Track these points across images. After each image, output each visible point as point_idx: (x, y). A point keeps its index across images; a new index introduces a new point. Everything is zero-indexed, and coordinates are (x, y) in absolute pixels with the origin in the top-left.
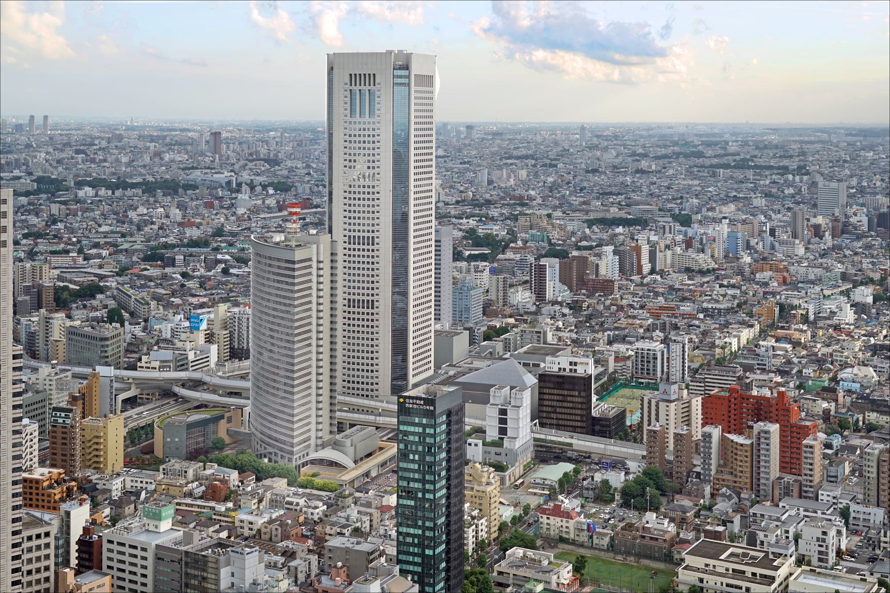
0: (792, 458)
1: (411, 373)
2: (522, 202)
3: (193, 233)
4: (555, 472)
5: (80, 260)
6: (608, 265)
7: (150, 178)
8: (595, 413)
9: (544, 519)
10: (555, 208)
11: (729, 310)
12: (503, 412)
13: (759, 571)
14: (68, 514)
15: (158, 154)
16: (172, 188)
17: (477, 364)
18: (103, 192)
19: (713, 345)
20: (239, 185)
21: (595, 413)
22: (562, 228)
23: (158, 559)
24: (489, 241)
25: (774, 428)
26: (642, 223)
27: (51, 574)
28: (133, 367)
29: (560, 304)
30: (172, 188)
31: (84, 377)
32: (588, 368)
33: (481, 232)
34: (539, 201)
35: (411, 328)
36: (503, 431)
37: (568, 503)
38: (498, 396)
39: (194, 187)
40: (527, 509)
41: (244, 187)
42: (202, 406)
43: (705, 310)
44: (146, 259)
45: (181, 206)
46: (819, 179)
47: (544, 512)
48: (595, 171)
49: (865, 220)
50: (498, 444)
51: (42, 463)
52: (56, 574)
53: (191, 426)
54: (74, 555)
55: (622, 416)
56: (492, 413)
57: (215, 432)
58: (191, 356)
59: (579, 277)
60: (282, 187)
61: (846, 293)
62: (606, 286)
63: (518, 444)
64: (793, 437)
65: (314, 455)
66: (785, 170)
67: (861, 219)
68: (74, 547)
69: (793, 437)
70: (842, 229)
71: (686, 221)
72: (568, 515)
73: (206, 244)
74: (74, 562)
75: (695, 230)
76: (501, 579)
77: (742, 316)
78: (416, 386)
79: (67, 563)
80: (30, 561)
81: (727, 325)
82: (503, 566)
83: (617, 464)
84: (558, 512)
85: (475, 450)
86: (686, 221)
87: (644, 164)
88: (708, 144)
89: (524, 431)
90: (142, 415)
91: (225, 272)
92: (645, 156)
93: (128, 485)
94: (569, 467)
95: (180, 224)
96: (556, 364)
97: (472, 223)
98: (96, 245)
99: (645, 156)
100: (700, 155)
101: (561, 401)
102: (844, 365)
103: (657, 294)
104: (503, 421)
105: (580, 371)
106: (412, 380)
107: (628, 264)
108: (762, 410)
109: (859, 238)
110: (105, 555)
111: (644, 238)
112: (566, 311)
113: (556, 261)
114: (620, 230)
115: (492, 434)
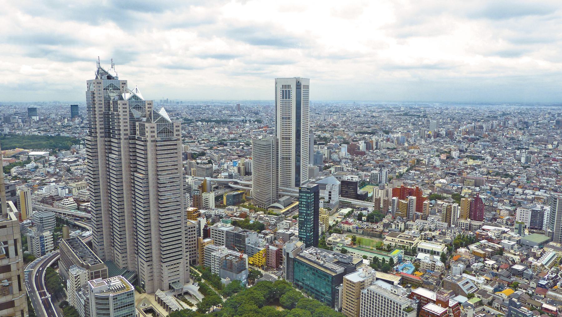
0: (420, 207)
1: (301, 180)
2: (335, 126)
3: (232, 136)
4: (346, 211)
5: (199, 145)
6: (362, 146)
7: (219, 119)
8: (359, 193)
9: (342, 225)
10: (345, 128)
11: (401, 161)
12: (330, 192)
13: (408, 241)
14: (200, 221)
15: (220, 111)
16: (225, 122)
17: (322, 177)
18: (204, 123)
19: (395, 172)
20: (246, 121)
21: (359, 193)
22: (348, 135)
23: (227, 235)
24: (325, 139)
25: (414, 198)
26: (373, 133)
27: (196, 239)
28: (216, 177)
29: (347, 159)
30: (225, 122)
31: (202, 180)
32: (356, 179)
33: (322, 136)
34: (340, 126)
35: (301, 166)
36: (330, 198)
37: (350, 220)
38: (328, 188)
39: (232, 122)
40: (337, 222)
41: (248, 122)
42: (238, 190)
43: (393, 161)
44: (219, 144)
45: (229, 128)
46: (430, 119)
47: (343, 223)
48: (358, 116)
49: (445, 133)
50: (329, 202)
51: (191, 206)
52: (198, 239)
53: (234, 196)
54: (202, 233)
55: (367, 194)
56: (327, 193)
57: (242, 198)
58: (234, 175)
59: (353, 150)
60: (259, 121)
61: (438, 156)
62: (363, 153)
63: (334, 203)
64: (420, 201)
65: (272, 205)
66: (419, 116)
67: (443, 132)
68: (202, 231)
69: (420, 201)
70: (437, 135)
71: (387, 133)
72: (350, 224)
73: (236, 140)
74: (202, 235)
75: (391, 136)
76: (329, 243)
77: (405, 163)
78: (303, 184)
79: (200, 236)
80: (190, 235)
81: (399, 166)
82: (330, 239)
83: (365, 209)
84: (347, 223)
85: (321, 205)
86: (387, 133)
87: (374, 114)
88: (395, 108)
89: (336, 198)
90: (220, 192)
91: (243, 148)
92: (374, 111)
93: (217, 213)
94: (349, 209)
95: (228, 133)
96: (347, 178)
97: (319, 133)
98: (203, 140)
99: (374, 111)
100: (392, 111)
101: (348, 189)
102: (437, 179)
103: (378, 156)
104: (330, 195)
105: (354, 180)
106: (302, 182)
107: (369, 146)
108: (411, 193)
109: (443, 138)
110: (211, 233)
111: (374, 138)
112: (349, 161)
113: (346, 145)
114: (366, 135)
115: (327, 199)
